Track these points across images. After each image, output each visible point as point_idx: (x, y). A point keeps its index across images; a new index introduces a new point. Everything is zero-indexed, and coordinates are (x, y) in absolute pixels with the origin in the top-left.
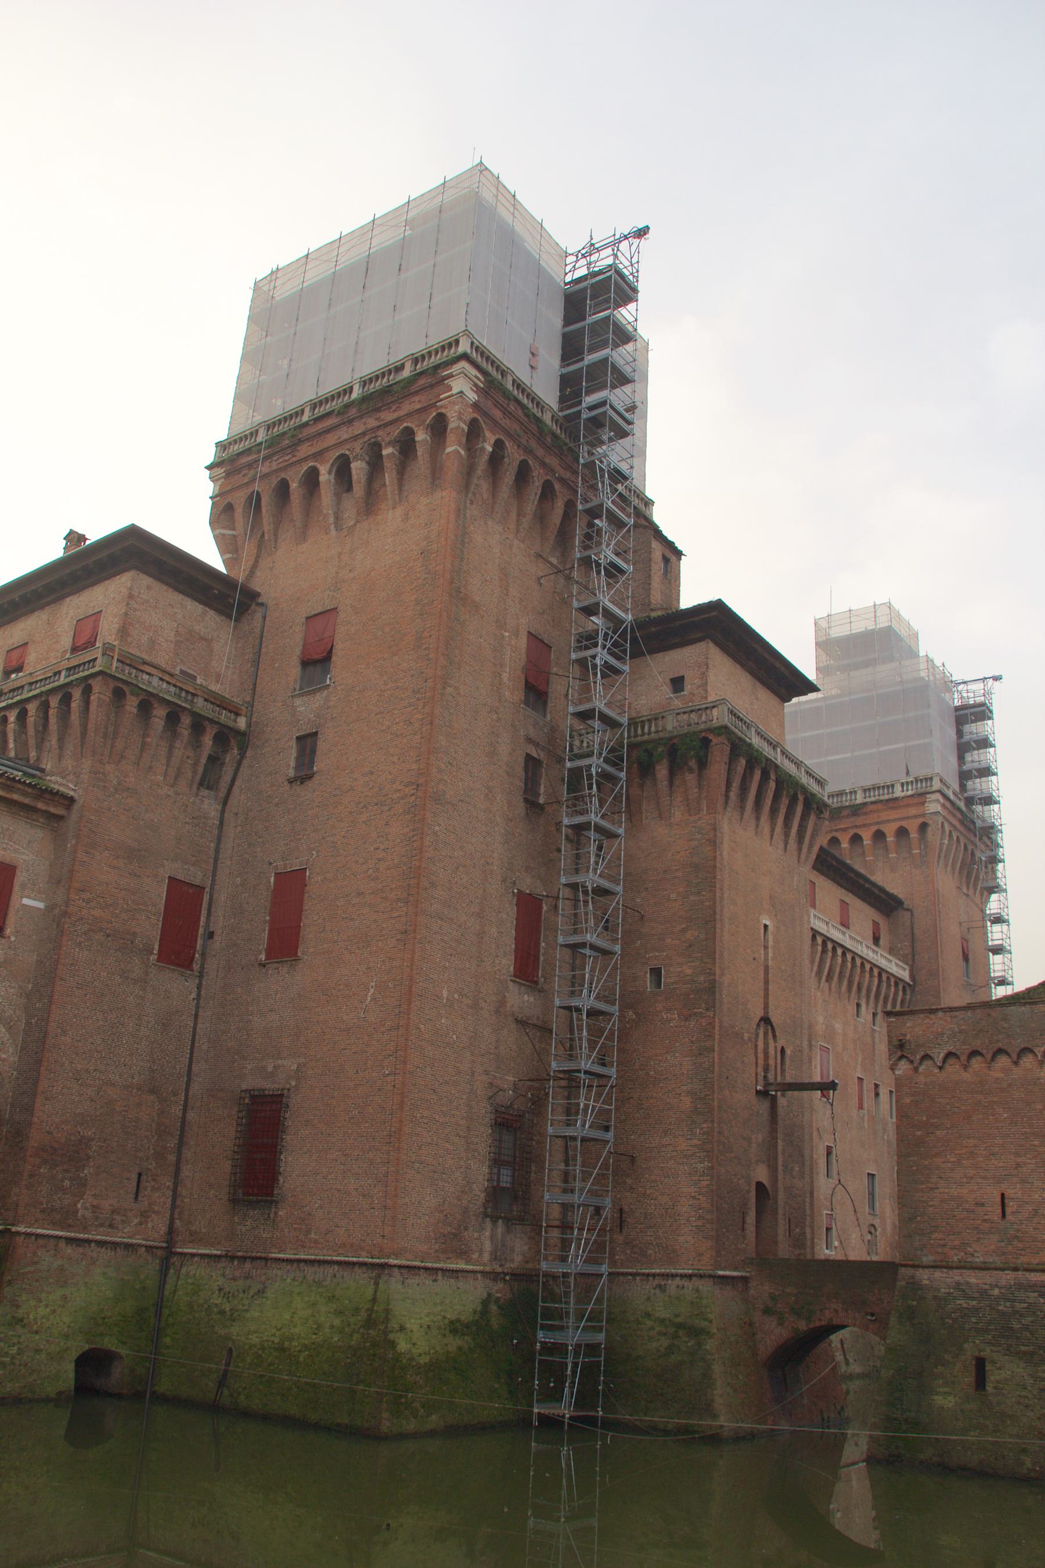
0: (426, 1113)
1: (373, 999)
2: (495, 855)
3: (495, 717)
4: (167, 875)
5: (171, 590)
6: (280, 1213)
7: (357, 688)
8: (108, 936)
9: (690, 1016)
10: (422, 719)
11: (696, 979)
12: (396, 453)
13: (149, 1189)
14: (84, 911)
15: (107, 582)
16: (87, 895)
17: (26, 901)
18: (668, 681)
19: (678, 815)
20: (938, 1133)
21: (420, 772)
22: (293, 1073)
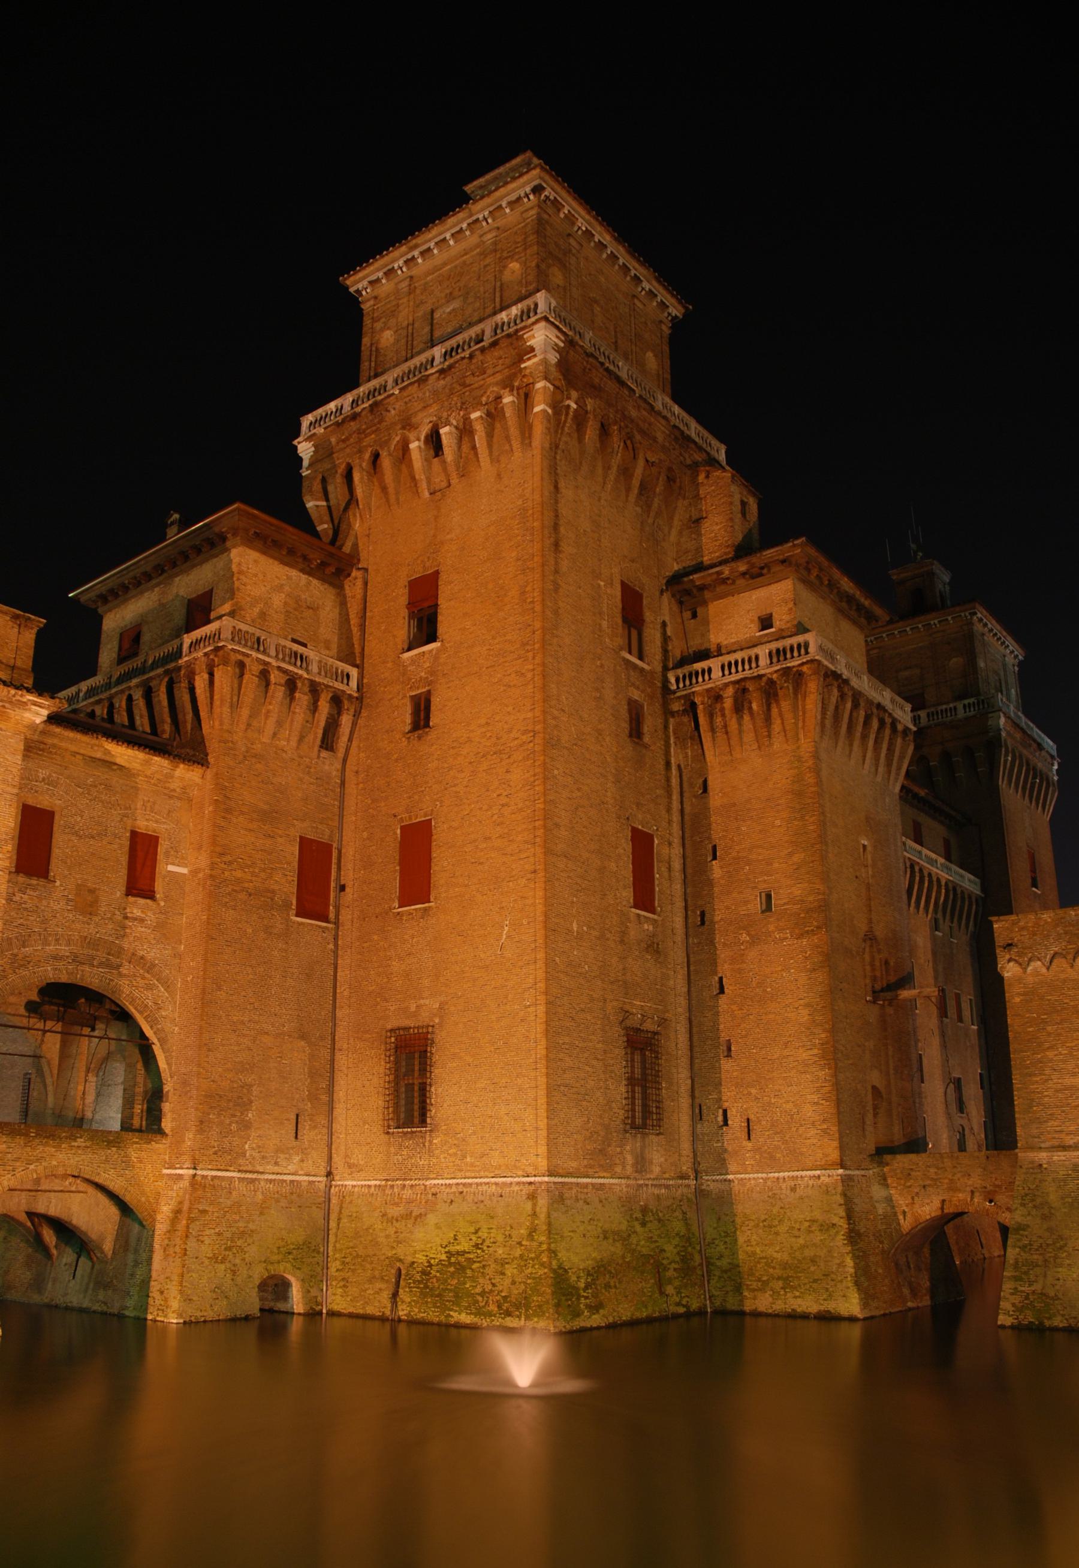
0: (567, 1040)
1: (508, 937)
2: (609, 794)
3: (598, 663)
4: (298, 835)
5: (276, 563)
6: (435, 1141)
7: (466, 645)
8: (250, 895)
9: (802, 935)
10: (533, 670)
11: (805, 899)
12: (484, 416)
13: (307, 1127)
14: (227, 873)
15: (215, 560)
16: (228, 858)
17: (171, 868)
18: (756, 619)
19: (778, 743)
20: (1049, 1028)
21: (536, 719)
22: (435, 1011)
